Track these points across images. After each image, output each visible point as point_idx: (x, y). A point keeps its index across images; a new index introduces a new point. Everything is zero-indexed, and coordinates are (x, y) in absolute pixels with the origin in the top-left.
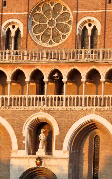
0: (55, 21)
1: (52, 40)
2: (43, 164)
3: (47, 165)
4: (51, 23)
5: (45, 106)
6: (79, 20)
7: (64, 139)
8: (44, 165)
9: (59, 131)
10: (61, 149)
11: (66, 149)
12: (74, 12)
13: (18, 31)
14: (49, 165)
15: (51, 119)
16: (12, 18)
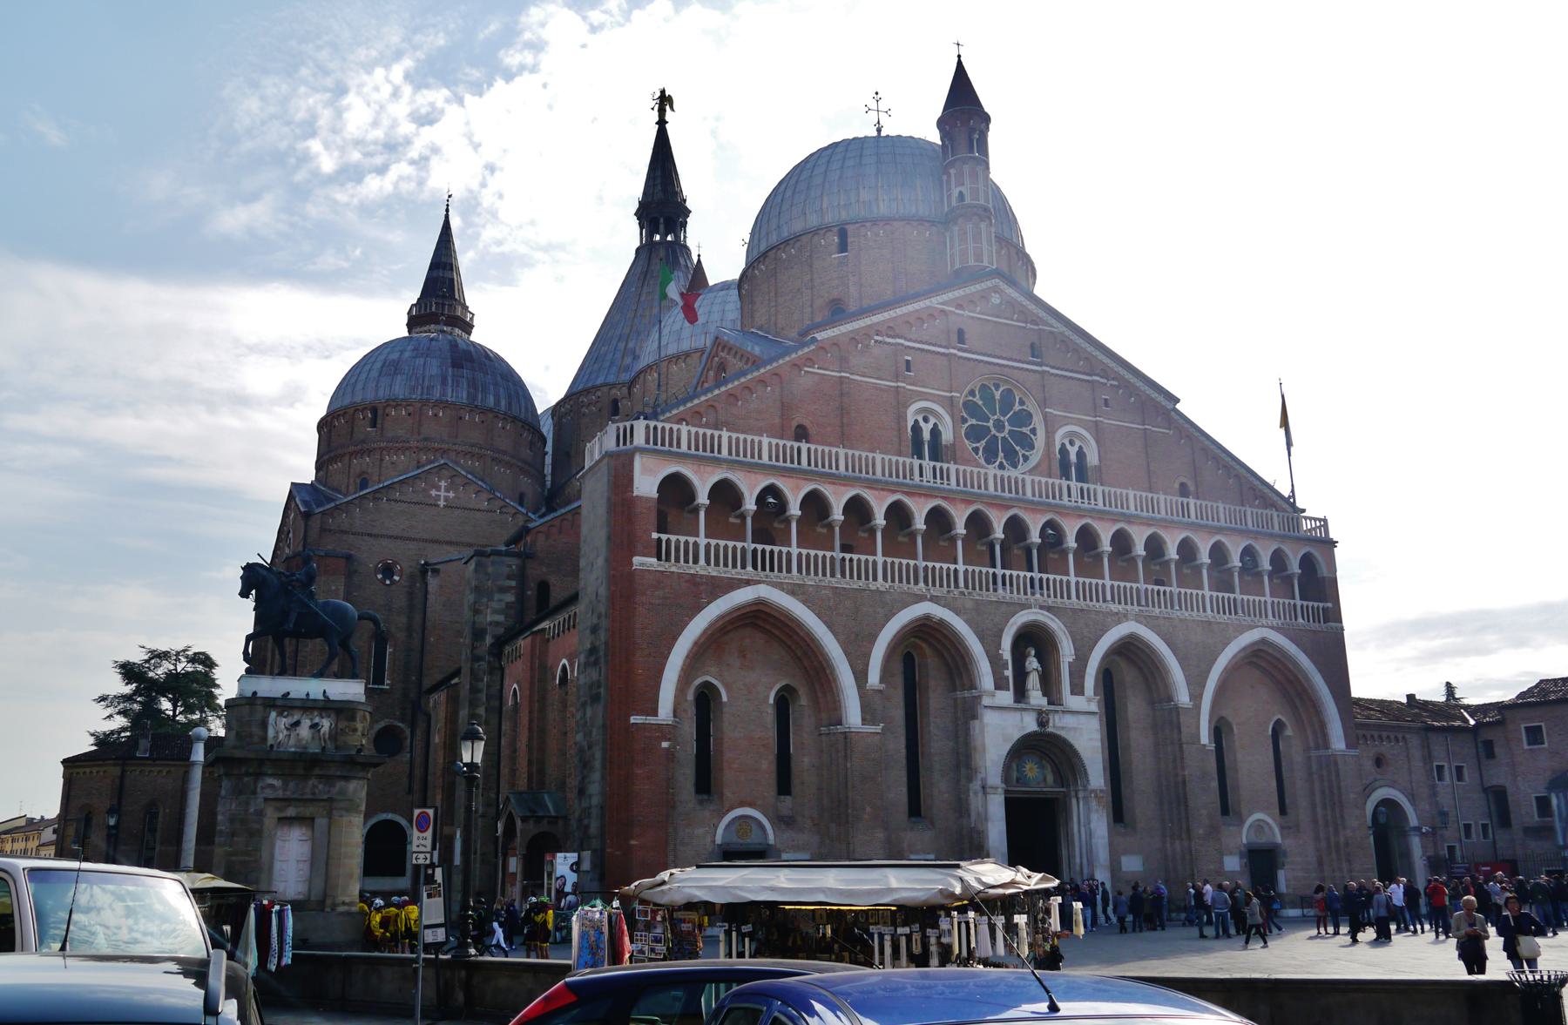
0: (1006, 424)
1: (1004, 461)
2: (1051, 724)
3: (1059, 727)
4: (999, 426)
5: (1038, 596)
6: (1057, 429)
7: (1085, 672)
8: (1054, 727)
9: (1076, 654)
10: (1082, 693)
11: (1092, 693)
12: (1047, 410)
13: (935, 432)
14: (1063, 728)
15: (1055, 625)
16: (927, 400)
